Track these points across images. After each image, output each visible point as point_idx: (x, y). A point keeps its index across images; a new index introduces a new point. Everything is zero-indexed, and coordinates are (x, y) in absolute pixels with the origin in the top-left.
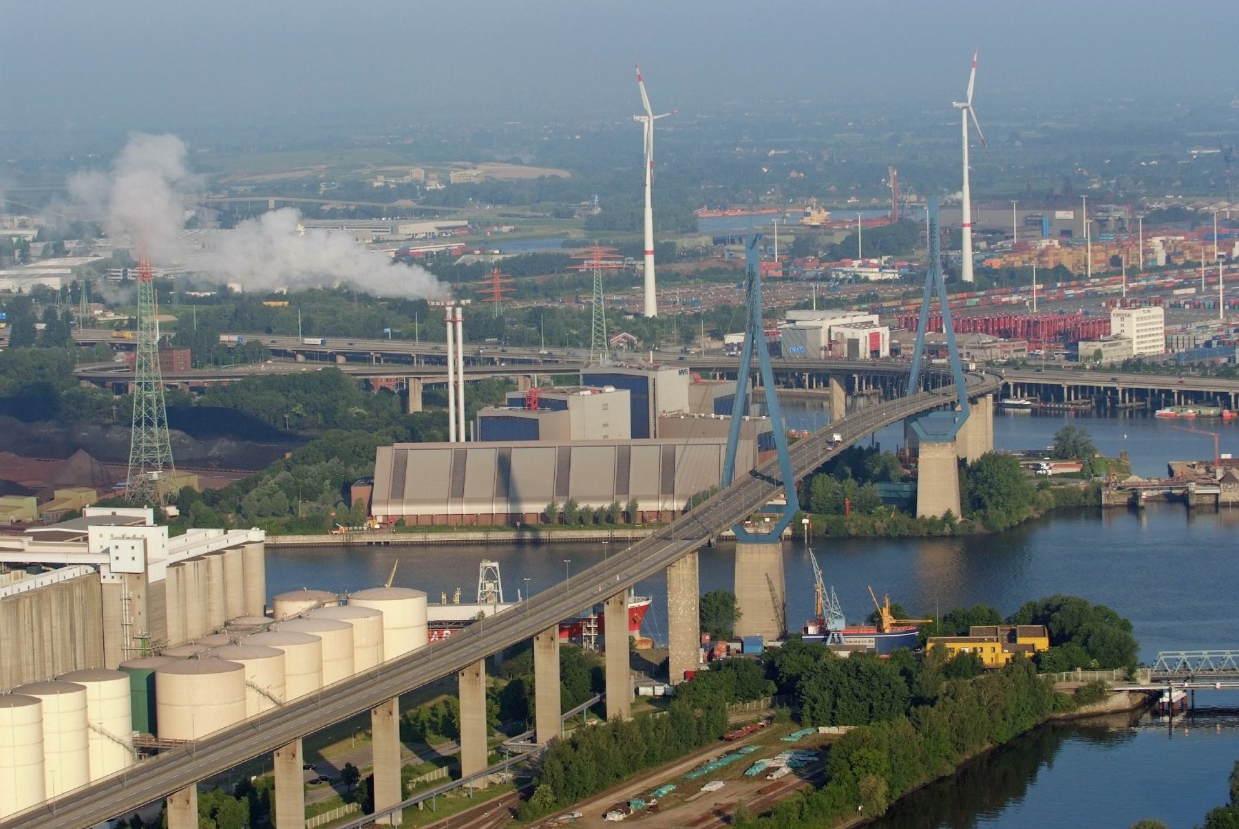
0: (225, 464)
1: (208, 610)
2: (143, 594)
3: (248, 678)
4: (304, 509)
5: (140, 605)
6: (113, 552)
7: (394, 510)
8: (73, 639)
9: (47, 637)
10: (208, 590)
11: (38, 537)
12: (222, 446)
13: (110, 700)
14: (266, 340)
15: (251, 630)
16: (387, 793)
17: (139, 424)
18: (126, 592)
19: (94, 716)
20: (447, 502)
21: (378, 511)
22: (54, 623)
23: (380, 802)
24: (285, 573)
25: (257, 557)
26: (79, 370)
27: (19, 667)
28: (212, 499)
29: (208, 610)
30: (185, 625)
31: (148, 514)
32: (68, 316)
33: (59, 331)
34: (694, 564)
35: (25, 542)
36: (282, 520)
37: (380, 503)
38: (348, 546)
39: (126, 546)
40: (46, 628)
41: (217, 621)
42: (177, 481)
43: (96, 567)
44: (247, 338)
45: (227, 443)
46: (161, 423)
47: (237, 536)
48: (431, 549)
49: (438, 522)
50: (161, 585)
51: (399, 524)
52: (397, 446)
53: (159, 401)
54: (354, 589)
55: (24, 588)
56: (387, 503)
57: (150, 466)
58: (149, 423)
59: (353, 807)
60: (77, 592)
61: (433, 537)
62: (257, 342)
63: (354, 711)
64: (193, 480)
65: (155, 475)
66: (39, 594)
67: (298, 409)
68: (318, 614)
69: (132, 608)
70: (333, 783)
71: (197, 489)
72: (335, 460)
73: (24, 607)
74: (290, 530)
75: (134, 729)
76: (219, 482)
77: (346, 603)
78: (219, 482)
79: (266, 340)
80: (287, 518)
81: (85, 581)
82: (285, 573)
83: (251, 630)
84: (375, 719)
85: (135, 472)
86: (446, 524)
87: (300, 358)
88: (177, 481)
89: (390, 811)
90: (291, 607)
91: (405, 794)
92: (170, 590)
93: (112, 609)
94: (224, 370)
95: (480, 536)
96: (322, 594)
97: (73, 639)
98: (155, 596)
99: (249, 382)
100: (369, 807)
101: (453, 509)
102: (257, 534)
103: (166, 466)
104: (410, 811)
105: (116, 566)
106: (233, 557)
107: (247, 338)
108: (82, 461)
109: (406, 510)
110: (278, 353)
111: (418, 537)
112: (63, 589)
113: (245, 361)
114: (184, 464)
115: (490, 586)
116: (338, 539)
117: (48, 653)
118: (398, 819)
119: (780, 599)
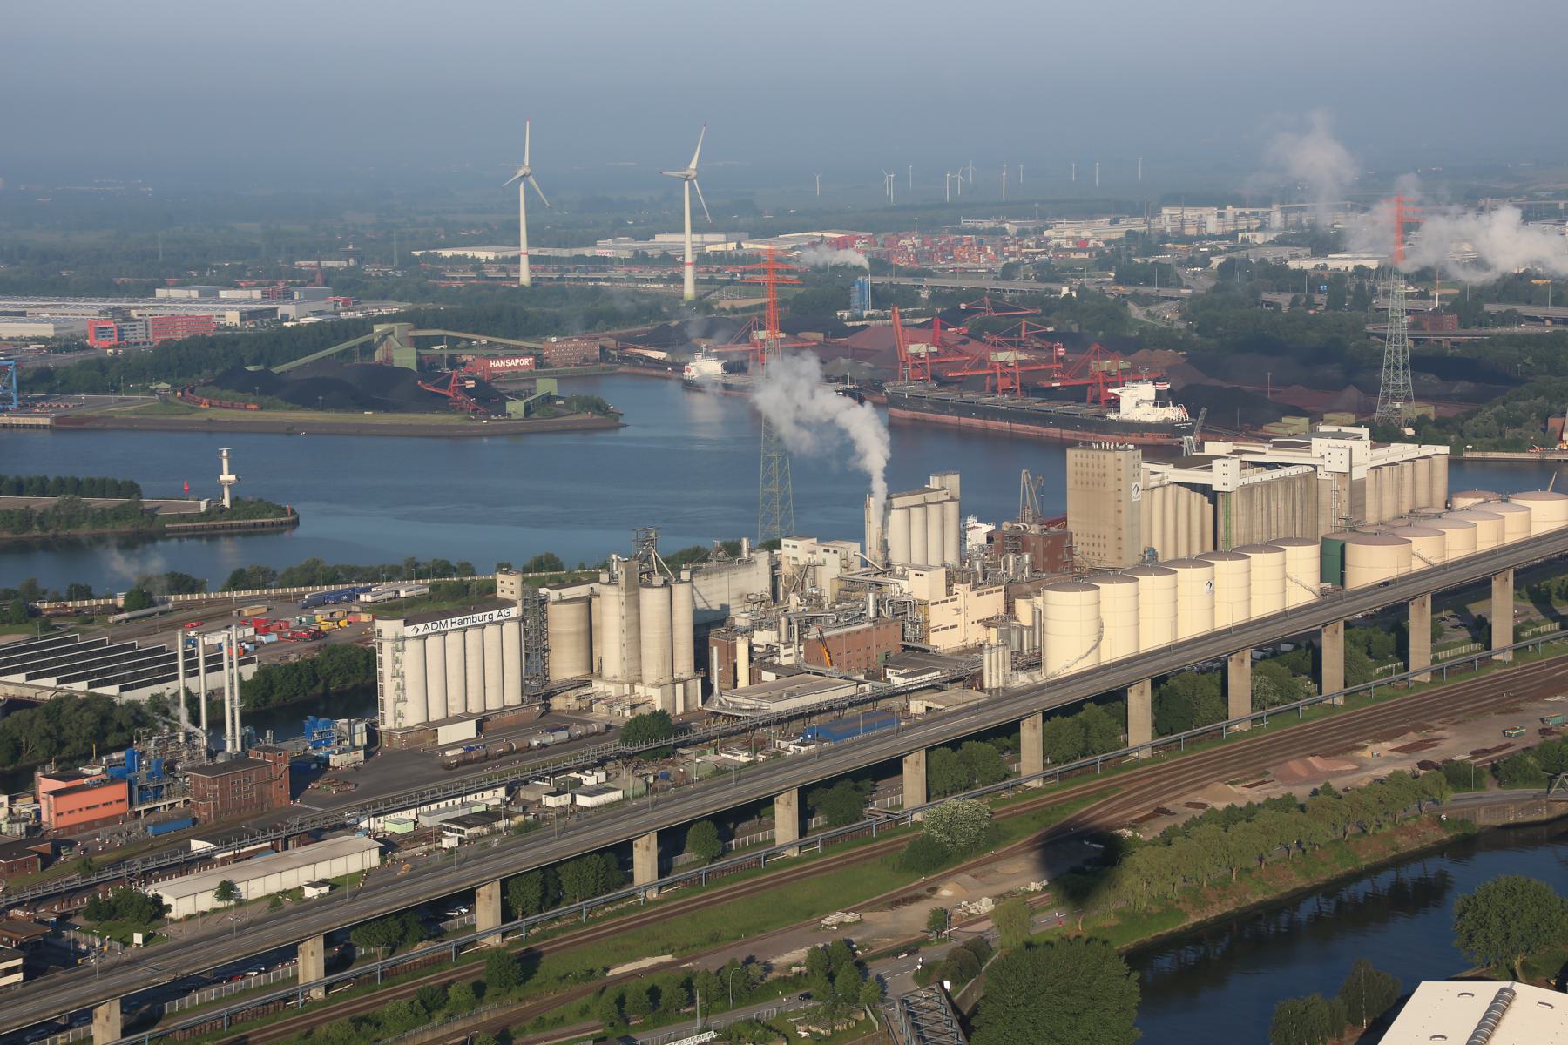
0: (1462, 399)
1: (1399, 502)
2: (1347, 486)
3: (1415, 550)
4: (1510, 433)
5: (1345, 495)
6: (1327, 457)
8: (1294, 517)
9: (1273, 515)
10: (1399, 487)
11: (1276, 445)
12: (1461, 387)
13: (1303, 561)
14: (1524, 309)
15: (1427, 517)
16: (1502, 635)
17: (1388, 367)
18: (1335, 486)
19: (1290, 570)
22: (1279, 504)
23: (1496, 644)
24: (1462, 476)
25: (1441, 465)
26: (1369, 329)
27: (1251, 535)
28: (1441, 424)
29: (1399, 502)
30: (1381, 509)
31: (1365, 431)
32: (1373, 289)
33: (1363, 298)
35: (1267, 448)
36: (1492, 441)
38: (1542, 462)
39: (1339, 453)
40: (1273, 509)
41: (1406, 509)
42: (1416, 410)
43: (1315, 467)
44: (1509, 307)
45: (1467, 384)
46: (1405, 367)
47: (1428, 450)
50: (1362, 482)
54: (1513, 492)
55: (1258, 479)
57: (1395, 399)
58: (1396, 367)
59: (1478, 646)
60: (1298, 484)
62: (1514, 311)
63: (1479, 576)
64: (1430, 410)
65: (1398, 405)
66: (1268, 485)
67: (1528, 360)
68: (1486, 508)
69: (1339, 497)
70: (1469, 629)
71: (1433, 418)
72: (1540, 399)
73: (1257, 493)
74: (1496, 448)
75: (1322, 581)
76: (1451, 411)
77: (1505, 501)
78: (1451, 411)
79: (1524, 309)
80: (1496, 439)
81: (1305, 477)
82: (1462, 476)
83: (1427, 517)
84: (1494, 584)
85: (1384, 402)
87: (1548, 323)
88: (1416, 410)
89: (1503, 650)
90: (1462, 502)
91: (1517, 638)
92: (1369, 486)
93: (1325, 496)
94: (1484, 331)
96: (1488, 494)
97: (1294, 517)
98: (1357, 489)
99: (1494, 341)
100: (1488, 646)
102: (1445, 449)
103: (1407, 399)
104: (1519, 651)
105: (1329, 467)
106: (1422, 466)
107: (1509, 307)
108: (1351, 394)
110: (1532, 319)
112: (1288, 482)
113: (1503, 324)
114: (1420, 397)
116: (1534, 457)
117: (1274, 526)
118: (1509, 657)
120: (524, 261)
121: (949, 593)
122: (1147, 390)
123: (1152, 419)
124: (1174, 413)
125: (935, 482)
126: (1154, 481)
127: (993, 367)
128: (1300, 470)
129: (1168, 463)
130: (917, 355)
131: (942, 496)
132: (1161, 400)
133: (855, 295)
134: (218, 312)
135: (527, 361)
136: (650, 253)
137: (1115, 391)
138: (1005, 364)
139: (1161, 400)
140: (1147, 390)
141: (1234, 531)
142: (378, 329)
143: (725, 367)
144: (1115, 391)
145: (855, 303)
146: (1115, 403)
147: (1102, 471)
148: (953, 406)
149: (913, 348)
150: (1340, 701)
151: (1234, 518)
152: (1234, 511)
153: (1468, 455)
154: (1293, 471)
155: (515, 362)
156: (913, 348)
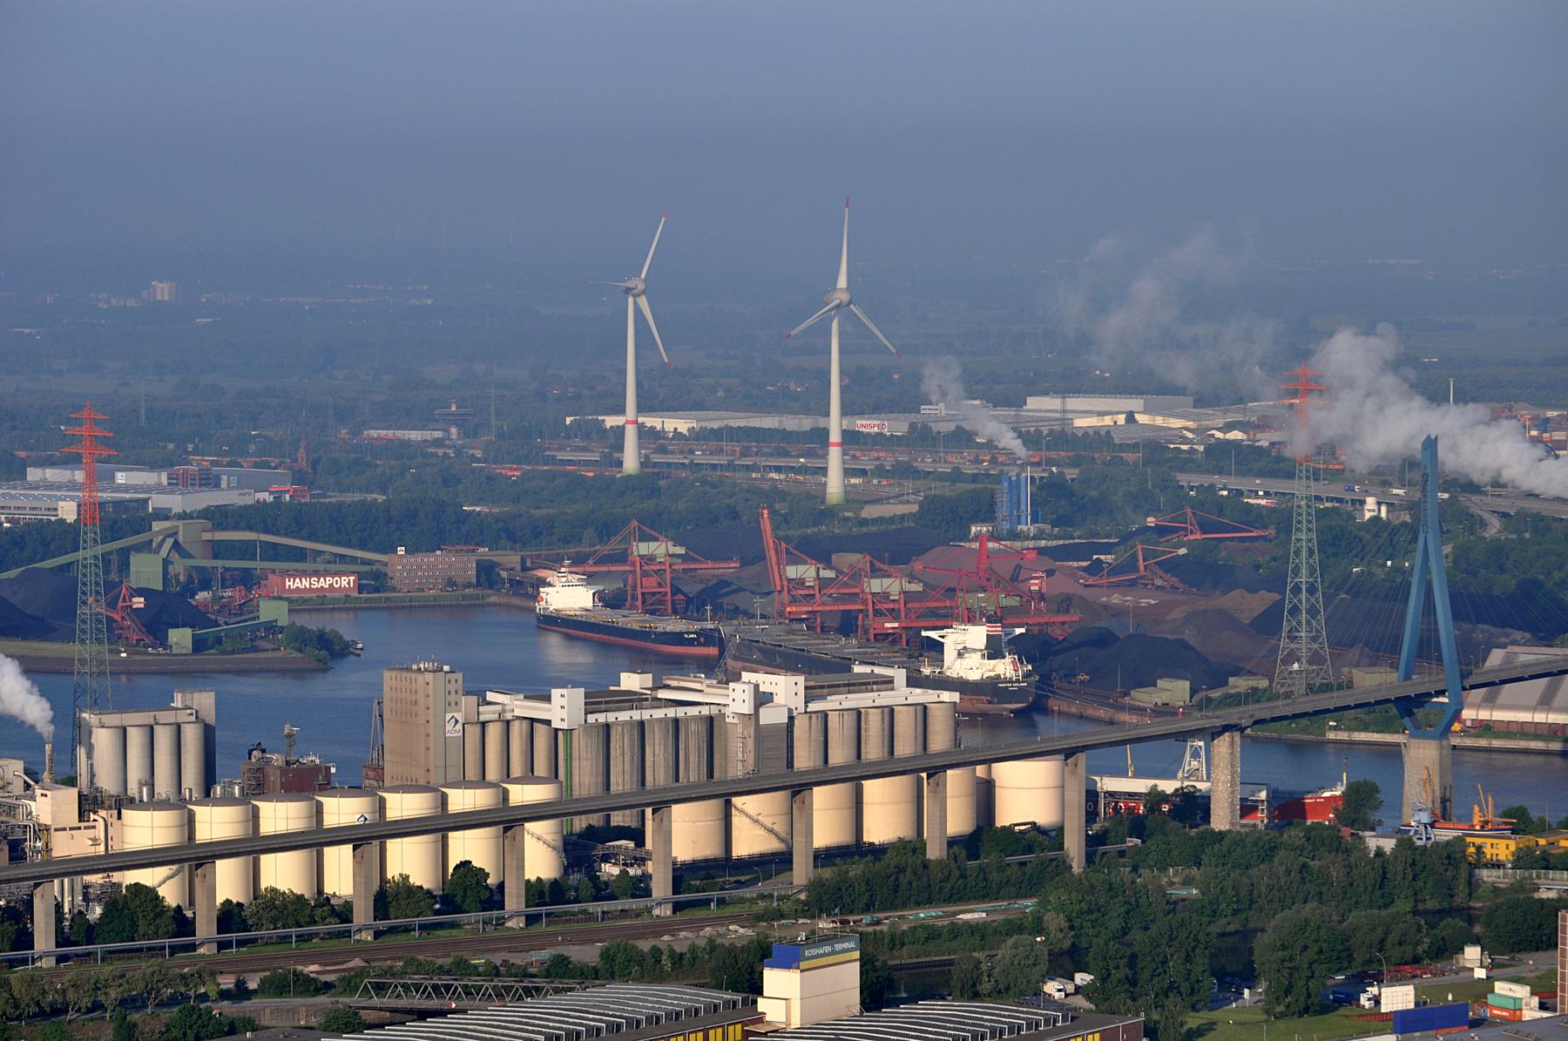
5: (751, 743)
7: (1484, 715)
20: (1534, 709)
21: (1468, 714)
34: (1232, 743)
37: (1472, 706)
48: (1495, 756)
49: (1514, 729)
51: (1485, 728)
52: (1510, 649)
53: (1312, 590)
56: (1478, 707)
60: (693, 727)
61: (1496, 743)
74: (1366, 729)
86: (1523, 730)
95: (1540, 745)
101: (1540, 717)
109: (1499, 715)
111: (1483, 743)
115: (1195, 764)
119: (1438, 794)
120: (631, 435)
121: (81, 817)
122: (977, 635)
123: (974, 676)
124: (1004, 667)
125: (178, 701)
126: (487, 713)
127: (865, 602)
128: (705, 711)
129: (518, 691)
130: (801, 582)
131: (183, 717)
132: (994, 650)
133: (1003, 500)
134: (49, 504)
135: (346, 582)
136: (935, 427)
137: (934, 635)
138: (886, 595)
139: (994, 650)
140: (977, 635)
141: (576, 779)
142: (157, 526)
143: (600, 596)
144: (934, 635)
145: (1003, 511)
146: (938, 647)
147: (414, 697)
148: (781, 654)
149: (792, 572)
150: (368, 936)
151: (576, 764)
152: (575, 754)
153: (1331, 736)
154: (693, 711)
155: (325, 583)
156: (792, 572)
